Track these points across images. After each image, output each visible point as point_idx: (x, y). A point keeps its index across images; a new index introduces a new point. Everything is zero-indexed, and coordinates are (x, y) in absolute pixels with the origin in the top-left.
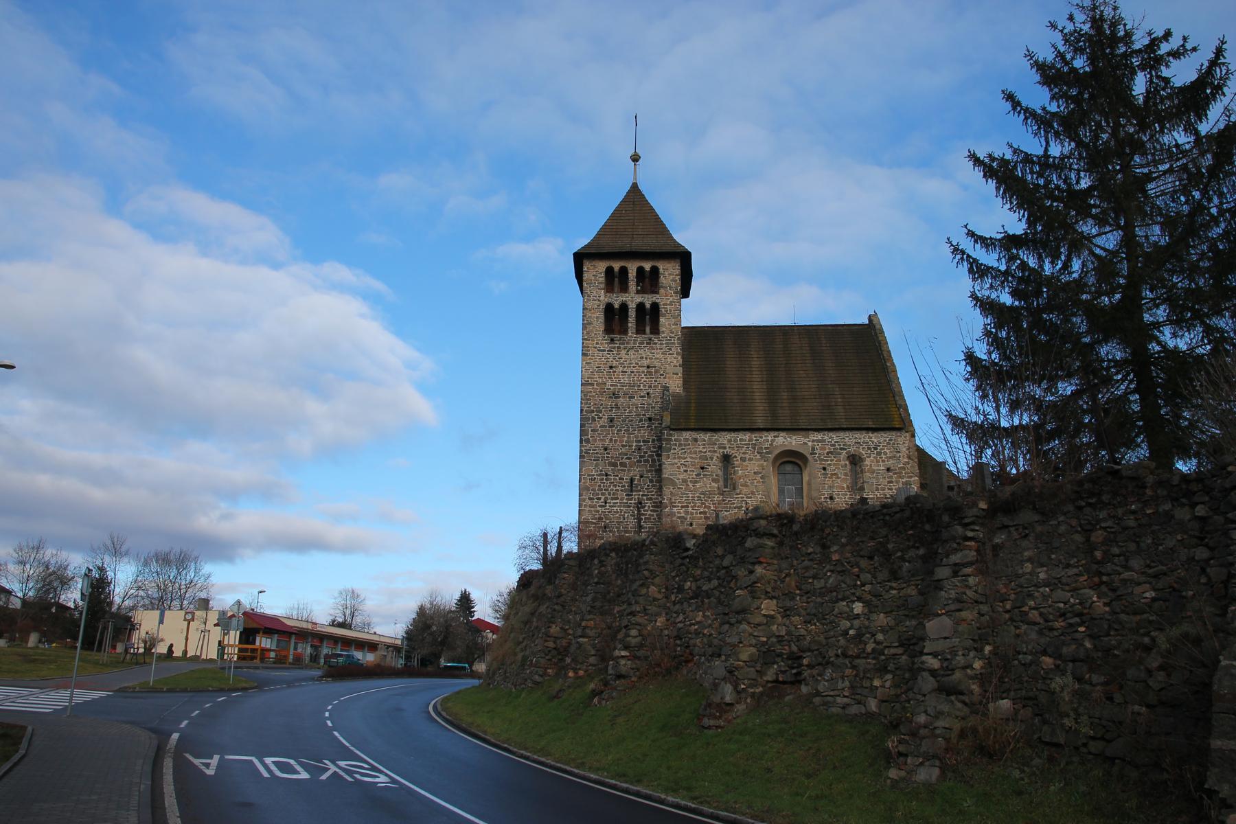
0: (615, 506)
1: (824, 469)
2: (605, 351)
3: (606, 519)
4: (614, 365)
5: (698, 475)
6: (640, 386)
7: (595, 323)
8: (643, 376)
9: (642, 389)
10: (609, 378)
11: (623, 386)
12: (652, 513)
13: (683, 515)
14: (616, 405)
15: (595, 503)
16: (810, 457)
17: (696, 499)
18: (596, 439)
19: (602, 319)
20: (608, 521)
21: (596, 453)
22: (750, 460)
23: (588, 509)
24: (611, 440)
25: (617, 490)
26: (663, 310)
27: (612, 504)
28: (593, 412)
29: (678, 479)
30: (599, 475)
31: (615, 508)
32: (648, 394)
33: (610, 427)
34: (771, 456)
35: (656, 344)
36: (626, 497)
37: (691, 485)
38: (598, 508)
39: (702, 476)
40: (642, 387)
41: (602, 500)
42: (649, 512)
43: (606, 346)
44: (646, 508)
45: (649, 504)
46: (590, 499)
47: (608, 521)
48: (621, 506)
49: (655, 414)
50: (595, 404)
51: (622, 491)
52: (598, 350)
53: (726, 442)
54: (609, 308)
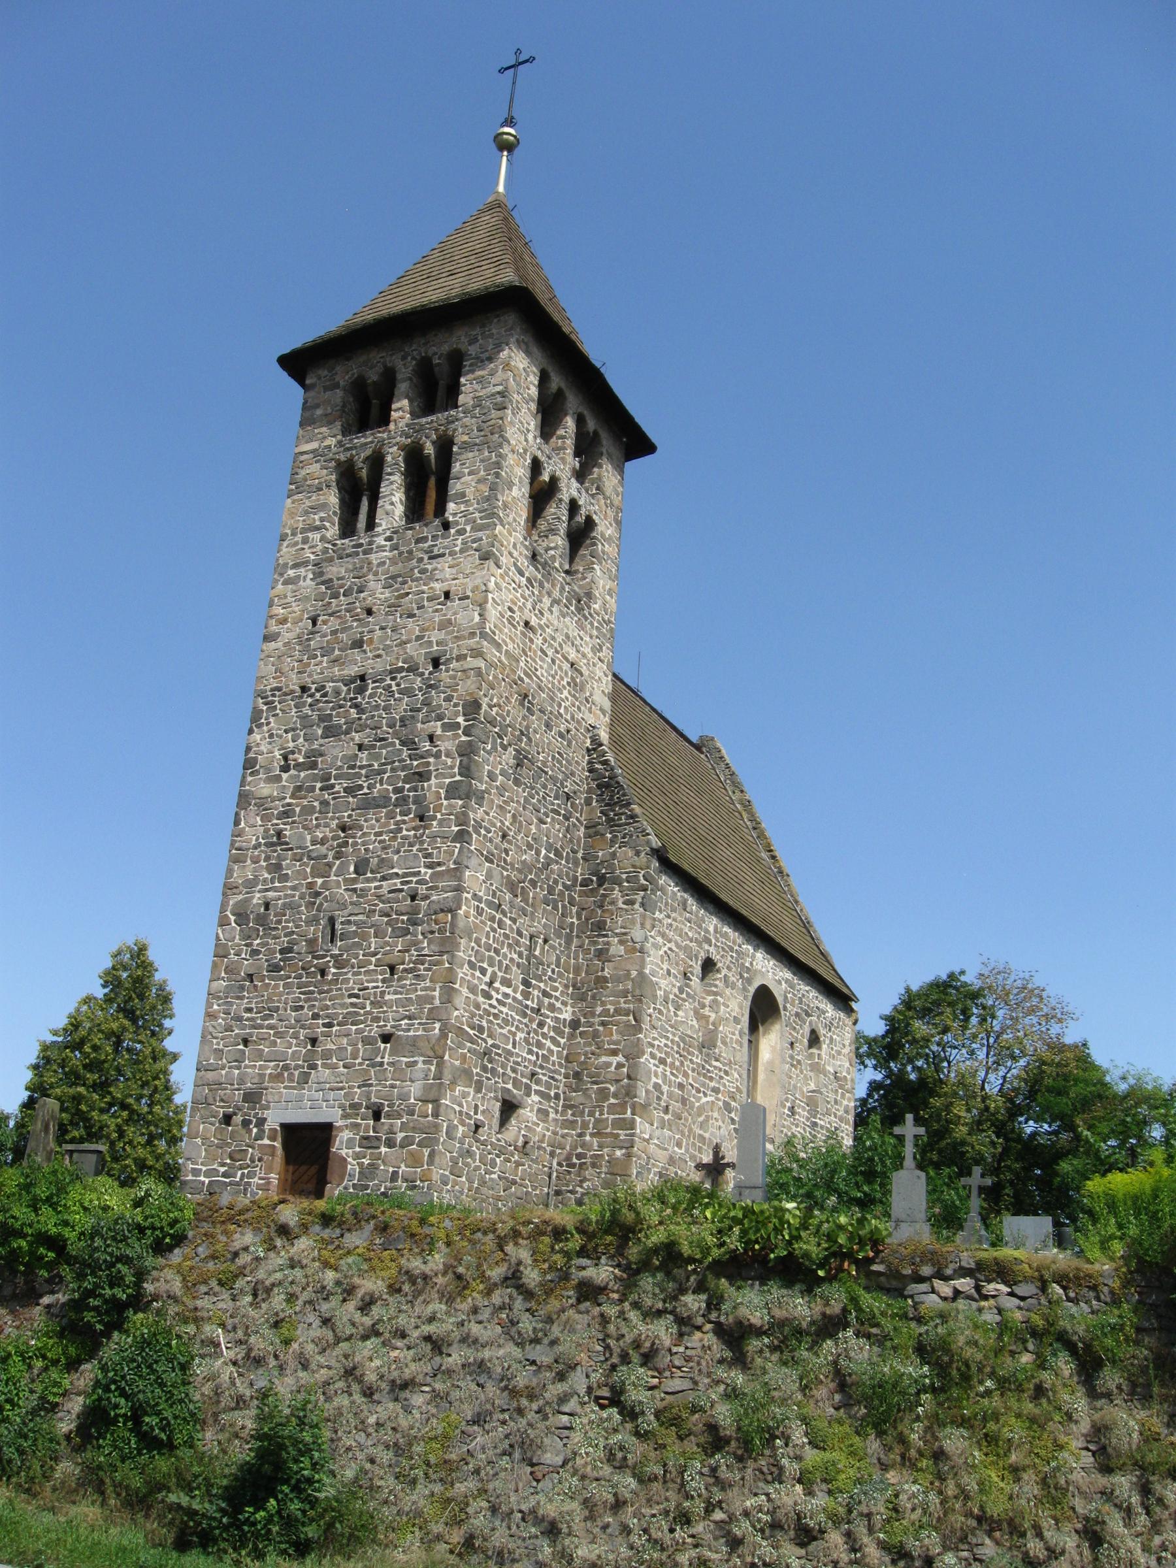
0: (504, 1004)
1: (792, 1044)
2: (523, 576)
3: (489, 1036)
4: (532, 623)
5: (681, 991)
6: (560, 706)
7: (515, 492)
8: (565, 683)
9: (561, 715)
10: (523, 650)
11: (540, 687)
12: (553, 1047)
13: (660, 1081)
14: (528, 728)
15: (476, 981)
16: (782, 1012)
17: (675, 1048)
18: (492, 801)
19: (526, 490)
20: (490, 1042)
21: (491, 841)
22: (733, 986)
23: (465, 991)
24: (514, 816)
25: (512, 960)
26: (600, 546)
27: (500, 997)
28: (493, 723)
29: (660, 988)
30: (490, 904)
31: (505, 1010)
32: (568, 731)
33: (517, 782)
34: (752, 990)
35: (586, 619)
36: (521, 987)
37: (672, 1009)
38: (481, 999)
39: (684, 996)
40: (562, 711)
41: (487, 979)
42: (548, 1043)
43: (524, 563)
44: (545, 1030)
45: (548, 1020)
46: (470, 962)
47: (490, 1042)
48: (511, 1008)
49: (575, 793)
50: (500, 706)
51: (518, 966)
52: (515, 565)
53: (711, 929)
54: (536, 466)
